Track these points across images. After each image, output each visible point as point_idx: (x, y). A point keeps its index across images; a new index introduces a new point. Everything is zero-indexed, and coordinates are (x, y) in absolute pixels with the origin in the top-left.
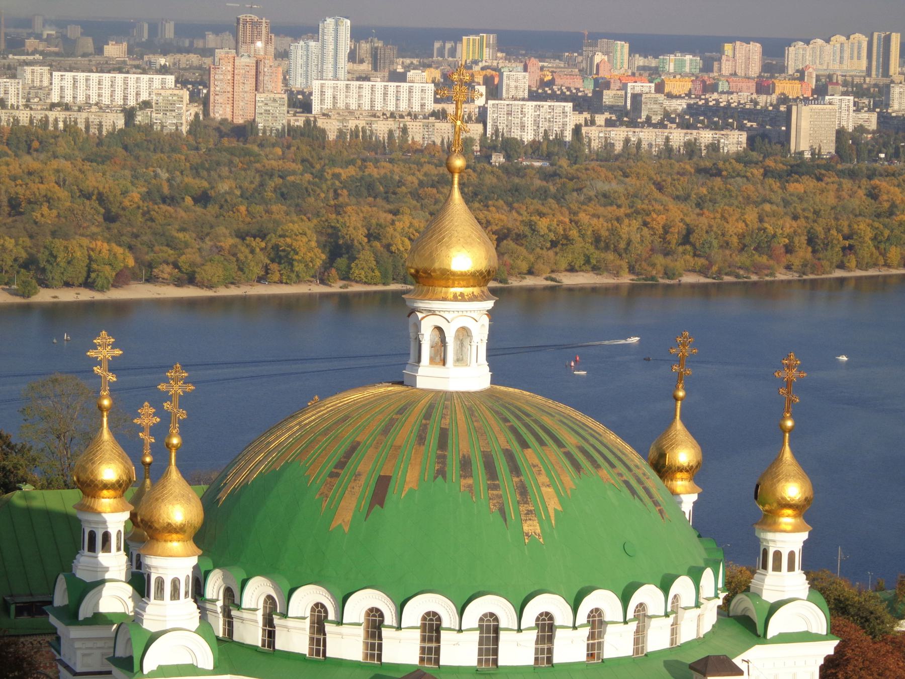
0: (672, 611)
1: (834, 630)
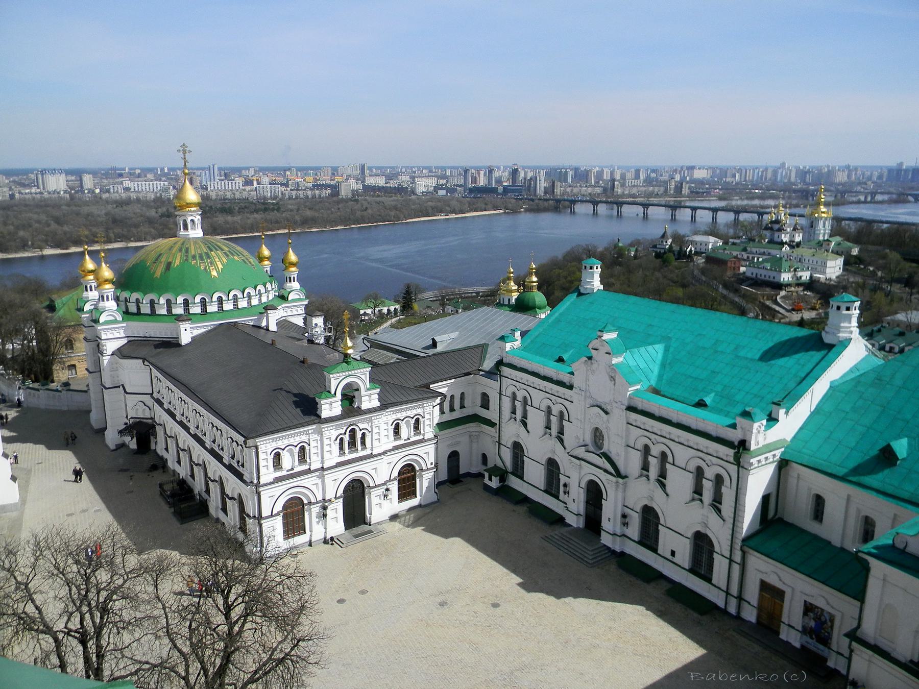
0: (260, 294)
1: (307, 297)
